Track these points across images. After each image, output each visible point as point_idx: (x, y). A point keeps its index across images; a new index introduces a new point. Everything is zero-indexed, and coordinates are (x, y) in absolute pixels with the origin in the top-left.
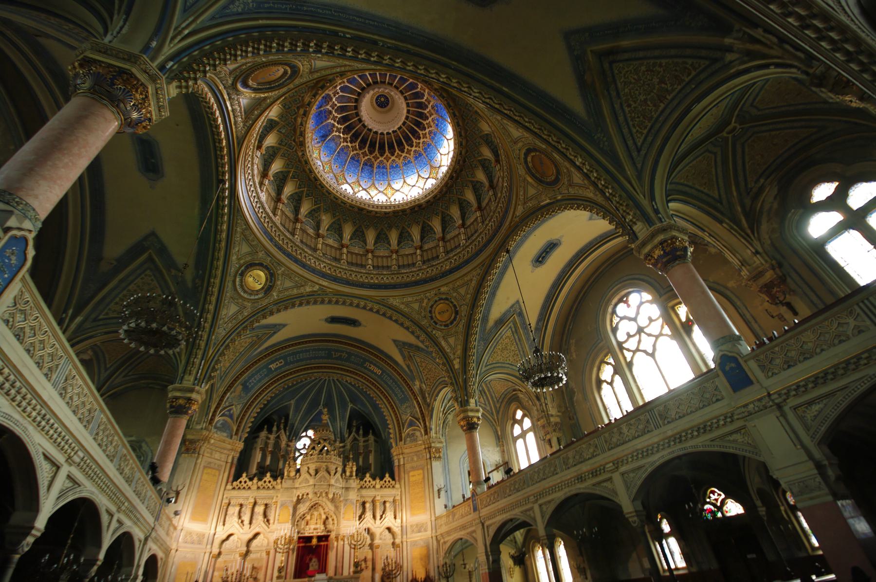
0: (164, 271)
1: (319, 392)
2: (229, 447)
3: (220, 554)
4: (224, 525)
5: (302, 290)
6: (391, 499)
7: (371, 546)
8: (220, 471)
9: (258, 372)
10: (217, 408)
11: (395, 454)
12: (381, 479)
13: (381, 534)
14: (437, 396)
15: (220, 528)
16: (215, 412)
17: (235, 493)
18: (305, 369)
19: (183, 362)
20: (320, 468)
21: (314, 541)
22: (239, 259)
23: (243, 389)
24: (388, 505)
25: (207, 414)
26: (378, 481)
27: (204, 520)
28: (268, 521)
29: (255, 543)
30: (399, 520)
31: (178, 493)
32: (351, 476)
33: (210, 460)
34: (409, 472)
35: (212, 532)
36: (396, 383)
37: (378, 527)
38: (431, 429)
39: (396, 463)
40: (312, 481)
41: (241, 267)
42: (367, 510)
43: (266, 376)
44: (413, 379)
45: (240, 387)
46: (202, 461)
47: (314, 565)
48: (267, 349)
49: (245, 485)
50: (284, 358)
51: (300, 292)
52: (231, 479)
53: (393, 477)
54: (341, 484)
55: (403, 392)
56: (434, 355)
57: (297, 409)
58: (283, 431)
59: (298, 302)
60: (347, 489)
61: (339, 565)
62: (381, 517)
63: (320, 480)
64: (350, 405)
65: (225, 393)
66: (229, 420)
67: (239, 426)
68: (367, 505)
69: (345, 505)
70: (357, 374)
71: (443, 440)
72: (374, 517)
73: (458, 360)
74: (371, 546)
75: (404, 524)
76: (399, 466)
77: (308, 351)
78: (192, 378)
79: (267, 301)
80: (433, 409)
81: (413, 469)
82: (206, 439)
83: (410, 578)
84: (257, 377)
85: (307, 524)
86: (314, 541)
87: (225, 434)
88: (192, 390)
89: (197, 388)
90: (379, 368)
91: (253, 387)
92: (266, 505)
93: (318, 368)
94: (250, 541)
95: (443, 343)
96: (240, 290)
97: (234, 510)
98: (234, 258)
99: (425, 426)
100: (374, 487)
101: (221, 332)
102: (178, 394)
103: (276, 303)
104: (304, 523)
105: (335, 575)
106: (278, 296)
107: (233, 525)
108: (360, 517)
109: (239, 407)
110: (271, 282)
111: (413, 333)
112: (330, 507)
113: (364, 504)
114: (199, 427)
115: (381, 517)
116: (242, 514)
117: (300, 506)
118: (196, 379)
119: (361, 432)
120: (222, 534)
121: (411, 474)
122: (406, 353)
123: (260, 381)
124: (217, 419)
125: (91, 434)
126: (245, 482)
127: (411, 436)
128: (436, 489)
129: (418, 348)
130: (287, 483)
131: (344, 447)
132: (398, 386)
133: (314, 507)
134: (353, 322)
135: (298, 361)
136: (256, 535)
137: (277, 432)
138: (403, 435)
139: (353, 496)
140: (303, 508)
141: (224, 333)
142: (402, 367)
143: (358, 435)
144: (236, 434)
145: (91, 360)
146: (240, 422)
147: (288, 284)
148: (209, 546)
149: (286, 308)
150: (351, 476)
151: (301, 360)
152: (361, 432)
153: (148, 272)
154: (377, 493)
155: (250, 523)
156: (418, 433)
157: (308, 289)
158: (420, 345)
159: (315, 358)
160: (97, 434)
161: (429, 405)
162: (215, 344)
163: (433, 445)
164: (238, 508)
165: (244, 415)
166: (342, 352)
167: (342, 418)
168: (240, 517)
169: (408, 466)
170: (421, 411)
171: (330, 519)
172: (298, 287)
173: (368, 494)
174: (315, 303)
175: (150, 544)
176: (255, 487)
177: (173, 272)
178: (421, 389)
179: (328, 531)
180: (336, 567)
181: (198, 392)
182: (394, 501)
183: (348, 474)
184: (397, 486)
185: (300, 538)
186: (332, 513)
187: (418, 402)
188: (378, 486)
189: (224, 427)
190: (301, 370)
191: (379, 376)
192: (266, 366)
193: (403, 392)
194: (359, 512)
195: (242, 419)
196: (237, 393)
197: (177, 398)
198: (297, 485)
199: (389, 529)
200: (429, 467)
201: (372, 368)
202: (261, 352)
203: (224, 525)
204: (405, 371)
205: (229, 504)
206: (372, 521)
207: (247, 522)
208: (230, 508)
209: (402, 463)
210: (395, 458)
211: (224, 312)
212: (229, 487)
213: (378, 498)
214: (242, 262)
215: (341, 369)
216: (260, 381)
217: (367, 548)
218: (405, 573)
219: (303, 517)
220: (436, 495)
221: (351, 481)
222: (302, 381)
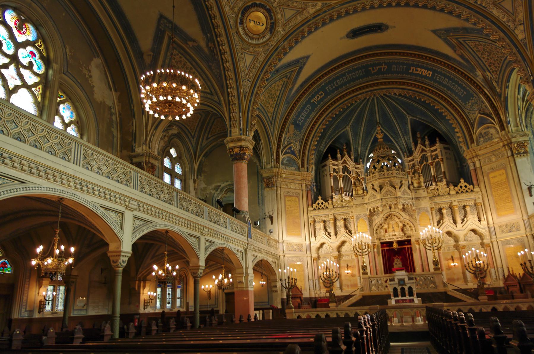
0: (184, 46)
1: (372, 113)
2: (299, 178)
3: (319, 257)
4: (315, 237)
5: (305, 14)
6: (472, 203)
7: (457, 247)
8: (298, 197)
9: (303, 109)
10: (278, 148)
11: (467, 158)
12: (455, 185)
13: (465, 235)
14: (508, 81)
15: (313, 239)
16: (278, 152)
17: (316, 213)
18: (347, 94)
19: (227, 118)
20: (384, 183)
21: (395, 246)
22: (232, 9)
23: (295, 128)
24: (468, 209)
25: (272, 155)
26: (452, 187)
27: (299, 235)
28: (350, 232)
29: (344, 248)
30: (484, 223)
31: (271, 218)
32: (420, 187)
34: (488, 174)
35: (308, 242)
36: (453, 80)
37: (461, 230)
38: (508, 123)
39: (472, 167)
40: (378, 196)
41: (237, 16)
42: (445, 215)
43: (312, 110)
44: (473, 70)
45: (292, 127)
46: (282, 193)
47: (397, 263)
48: (302, 85)
49: (323, 206)
50: (323, 89)
51: (304, 17)
52: (310, 202)
53: (471, 183)
54: (411, 194)
55: (464, 88)
56: (485, 32)
57: (356, 134)
58: (347, 156)
59: (306, 29)
60: (417, 199)
61: (425, 263)
62: (463, 220)
63: (386, 194)
64: (409, 118)
65: (281, 135)
66: (292, 156)
67: (303, 160)
68: (444, 211)
69: (419, 213)
70: (404, 84)
71: (528, 132)
72: (455, 222)
73: (522, 27)
74: (457, 247)
75: (491, 225)
76: (475, 169)
77: (344, 75)
78: (237, 130)
79: (275, 39)
80: (506, 99)
81: (493, 170)
82: (278, 175)
83: (506, 274)
84: (304, 114)
85: (386, 232)
86: (395, 246)
87: (293, 168)
88: (240, 140)
89: (243, 137)
90: (427, 69)
91: (303, 124)
92: (345, 219)
93: (360, 89)
94: (339, 248)
95: (495, 12)
96: (246, 39)
97: (320, 226)
98: (227, 9)
99: (500, 121)
100: (449, 194)
101: (246, 84)
102: (231, 145)
103: (286, 38)
104: (382, 231)
105: (423, 271)
106: (284, 30)
107: (322, 237)
108: (439, 222)
110: (271, 19)
111: (450, 13)
112: (404, 216)
113: (440, 210)
114: (269, 166)
115: (463, 220)
116: (327, 228)
117: (375, 217)
118: (240, 130)
119: (427, 143)
120: (315, 243)
121: (491, 175)
122: (454, 41)
123: (308, 116)
124: (281, 157)
125: (135, 188)
126: (322, 203)
127: (485, 136)
128: (525, 188)
129: (465, 30)
130: (359, 200)
131: (412, 160)
132: (457, 83)
133: (388, 217)
134: (378, 28)
135: (337, 88)
136: (343, 243)
137: (342, 158)
138: (474, 137)
139: (425, 204)
140: (378, 220)
141: (249, 84)
142: (455, 60)
143: (424, 145)
144: (303, 166)
145: (179, 133)
146: (303, 156)
147: (289, 13)
148: (308, 252)
149: (297, 42)
150: (420, 187)
151: (341, 86)
152: (427, 143)
153: (175, 52)
154: (453, 199)
155: (336, 234)
156: (492, 131)
157: (311, 10)
158: (468, 25)
159: (353, 80)
160: (143, 188)
161: (500, 96)
162: (245, 96)
163: (513, 140)
164: (322, 224)
165: (304, 150)
166: (380, 64)
167: (405, 133)
168: (326, 230)
169: (486, 168)
170: (492, 104)
171: (408, 227)
172: (300, 13)
173: (444, 201)
174: (324, 24)
175: (250, 253)
176: (330, 207)
177: (190, 44)
178: (485, 79)
179: (408, 237)
180: (422, 265)
181: (245, 140)
182: (475, 205)
183: (416, 185)
184: (477, 189)
185: (382, 243)
186: (407, 221)
187: (485, 95)
188: (453, 192)
189: (290, 163)
190: (344, 96)
191: (431, 79)
192: (308, 102)
193: (464, 88)
194: (437, 218)
195: (303, 153)
196: (291, 132)
197: (232, 148)
198: (367, 201)
199: (474, 231)
200: (512, 165)
201: (420, 71)
202: (298, 90)
203: (315, 237)
204: (459, 64)
205: (315, 221)
206: (453, 225)
207: (332, 233)
208: (317, 224)
209: (478, 165)
210: (469, 161)
211: (241, 65)
212: (310, 208)
213: (454, 204)
214: (236, 10)
215: (385, 83)
216: (308, 116)
217: (452, 249)
218: (500, 270)
219: (381, 226)
220: (526, 193)
221: (421, 191)
222: (349, 107)
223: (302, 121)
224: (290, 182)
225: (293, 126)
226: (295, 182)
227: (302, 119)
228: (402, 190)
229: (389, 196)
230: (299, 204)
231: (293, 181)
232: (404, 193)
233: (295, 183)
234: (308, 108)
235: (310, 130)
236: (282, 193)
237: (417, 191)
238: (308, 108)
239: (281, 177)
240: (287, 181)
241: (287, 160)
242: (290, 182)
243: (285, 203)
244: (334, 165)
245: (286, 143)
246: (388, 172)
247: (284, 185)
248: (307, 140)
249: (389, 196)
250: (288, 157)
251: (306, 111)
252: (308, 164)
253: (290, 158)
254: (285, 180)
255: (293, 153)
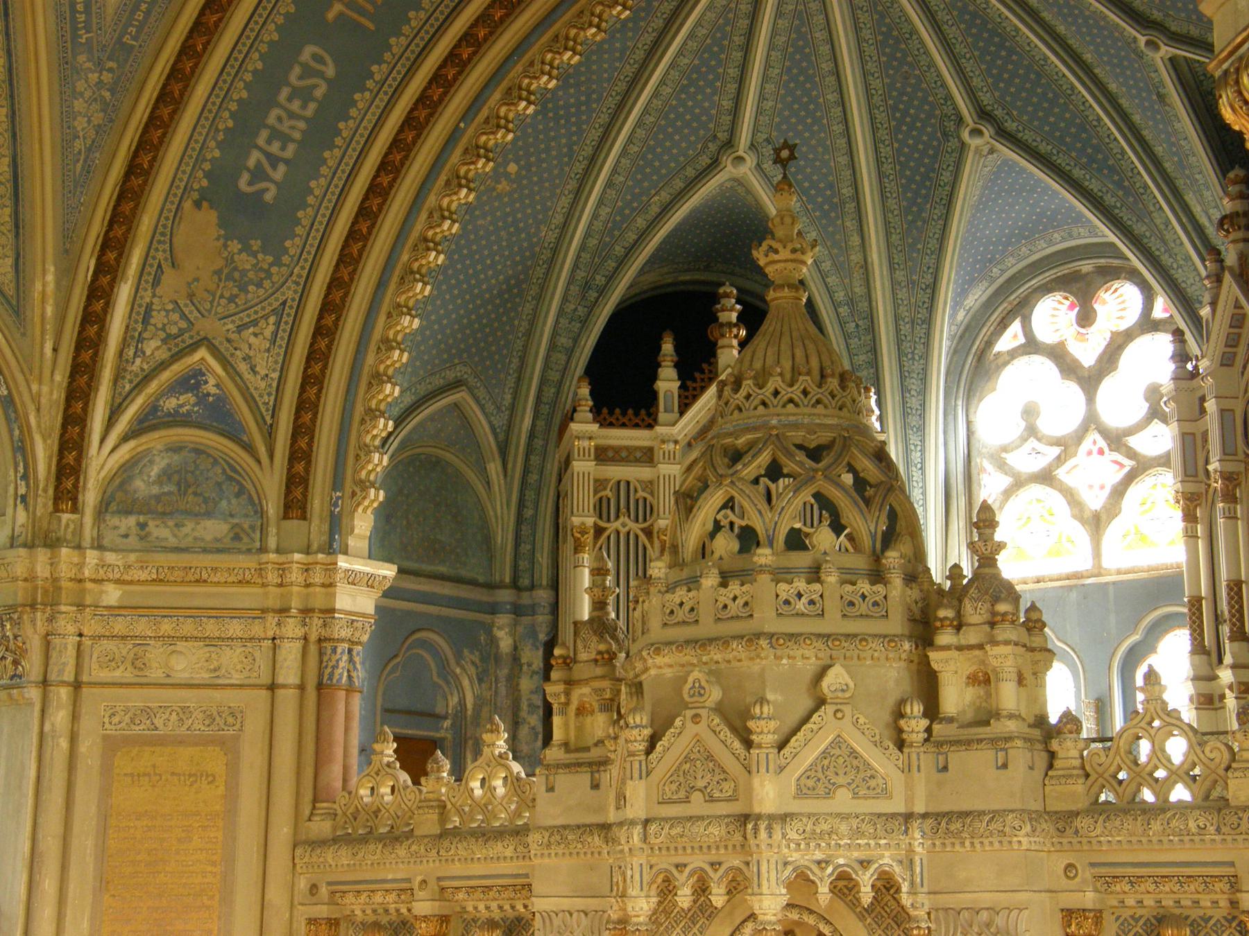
2: (249, 597)
8: (230, 747)
9: (268, 84)
33: (136, 699)
45: (202, 225)
54: (902, 784)
65: (99, 294)
67: (300, 455)
82: (45, 598)
84: (289, 116)
87: (214, 529)
109: (257, 344)
123: (321, 133)
124: (102, 460)
144: (295, 506)
146: (303, 430)
165: (313, 381)
183: (955, 697)
195: (307, 406)
216: (321, 133)
223: (279, 173)
224: (170, 639)
225: (209, 217)
226: (211, 628)
227: (274, 161)
228: (810, 756)
229: (697, 805)
230: (232, 795)
231: (188, 627)
232: (839, 765)
233: (210, 642)
234: (308, 72)
235: (353, 235)
236: (87, 724)
237: (956, 758)
238: (308, 72)
239: (81, 606)
240: (142, 627)
241: (166, 475)
242: (170, 639)
243: (106, 792)
244: (603, 455)
245: (150, 346)
246: (725, 595)
247: (110, 661)
248: (332, 307)
249: (697, 805)
250: (175, 449)
251: (305, 95)
252: (337, 482)
253: (198, 451)
254: (119, 626)
255: (218, 416)
